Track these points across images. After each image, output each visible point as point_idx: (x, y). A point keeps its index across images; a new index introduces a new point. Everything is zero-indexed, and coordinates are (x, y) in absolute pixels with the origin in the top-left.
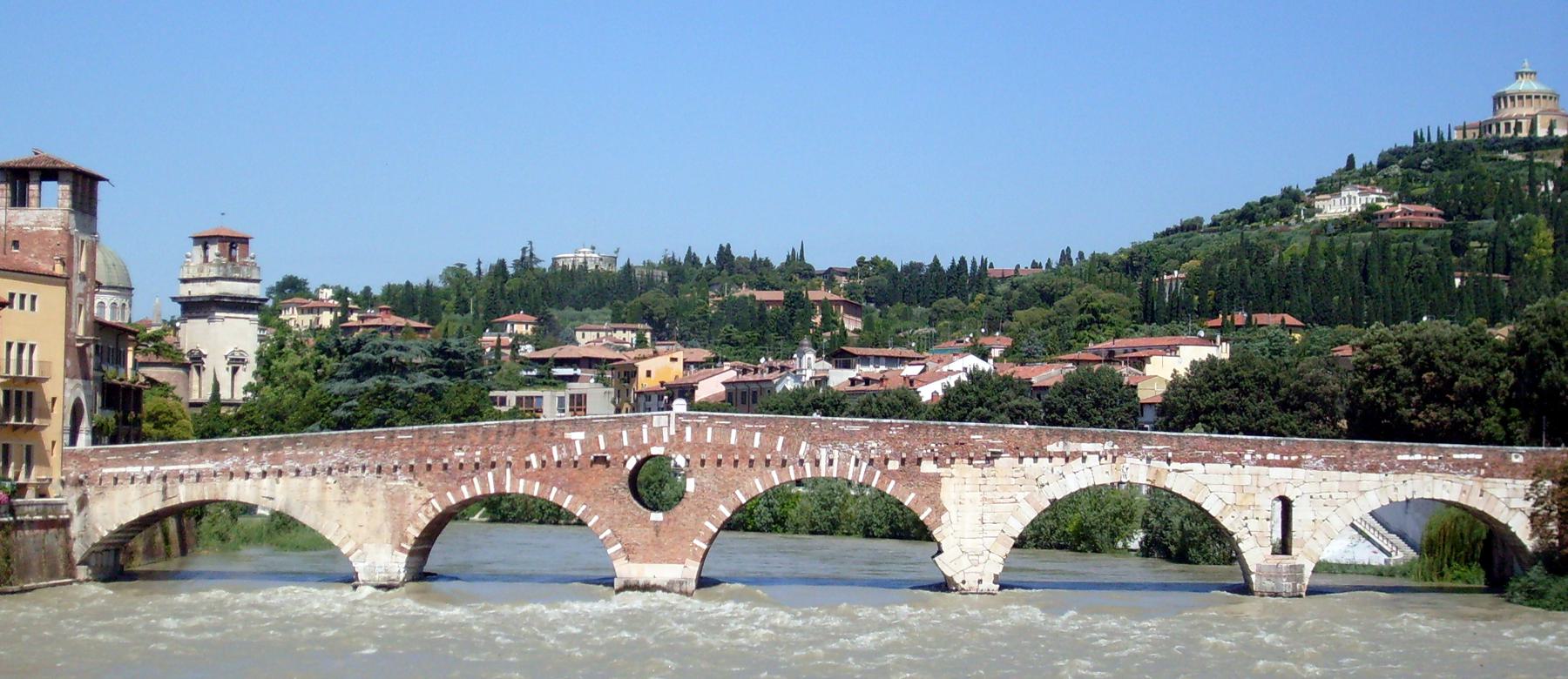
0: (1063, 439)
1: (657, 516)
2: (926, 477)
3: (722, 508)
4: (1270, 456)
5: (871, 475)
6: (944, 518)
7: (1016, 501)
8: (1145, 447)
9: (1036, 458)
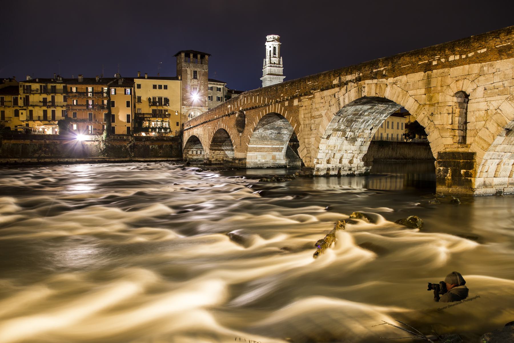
0: (339, 76)
4: (451, 58)
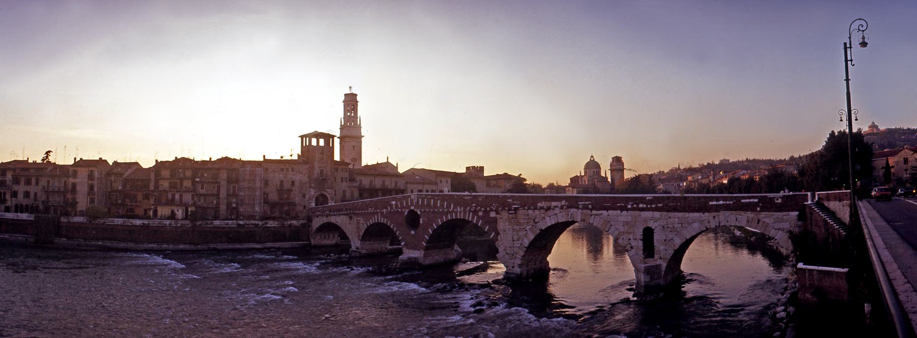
1: (413, 232)
3: (430, 230)
4: (641, 206)
5: (473, 218)
6: (499, 237)
7: (526, 230)
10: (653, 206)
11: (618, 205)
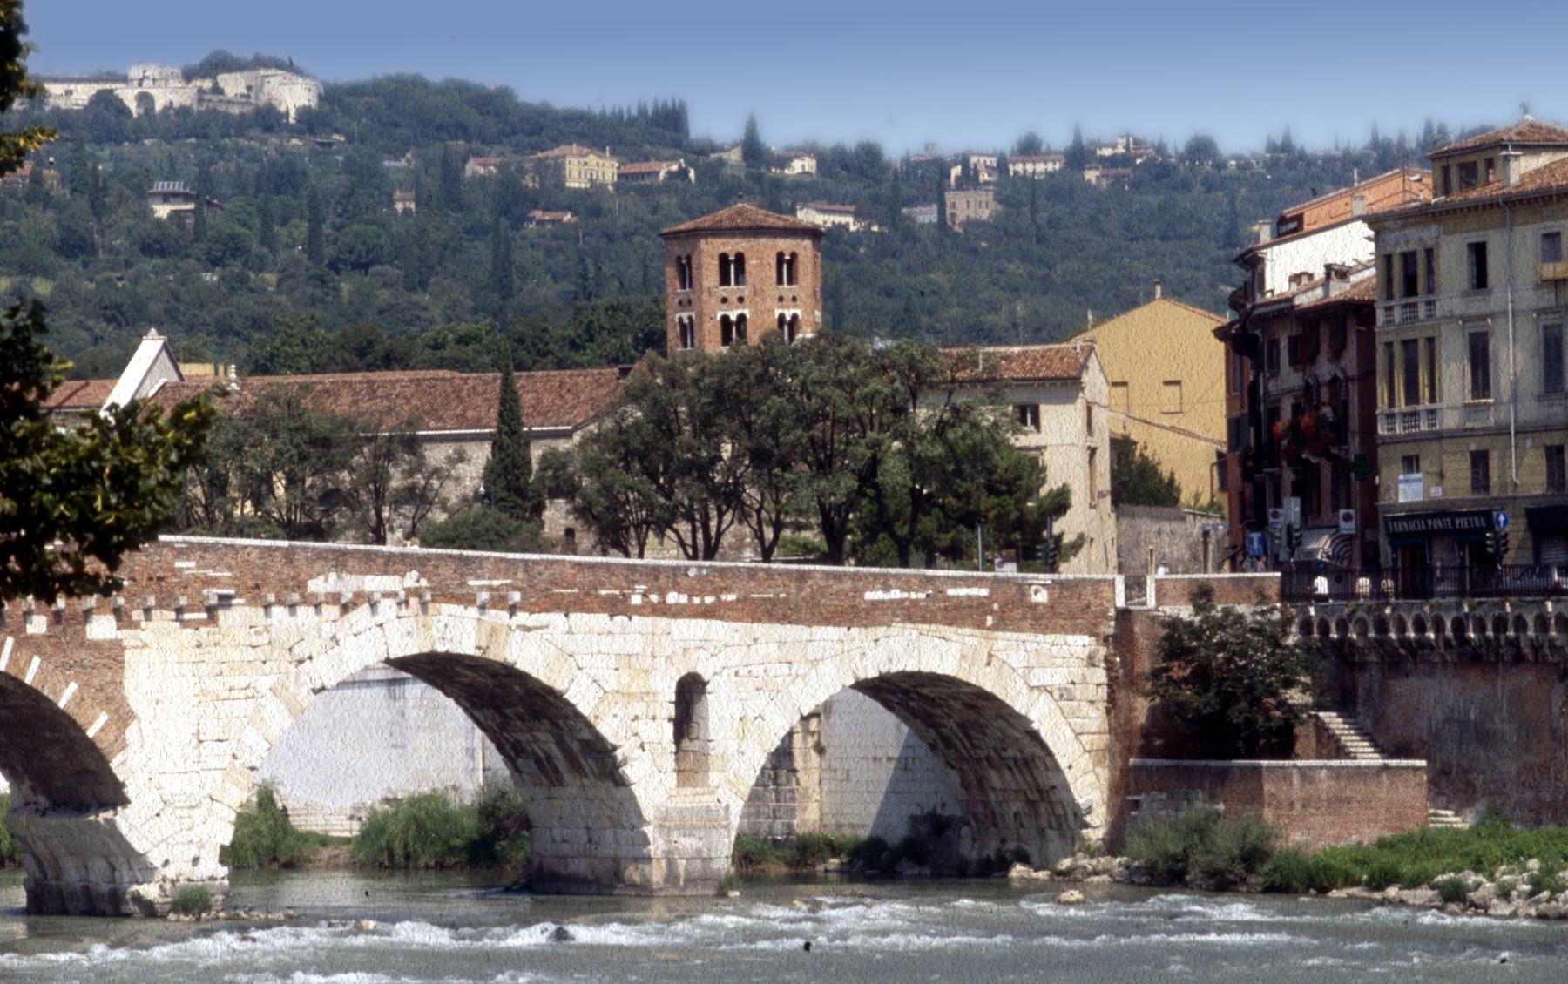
2: (97, 646)
4: (673, 598)
6: (131, 732)
8: (472, 582)
9: (292, 607)
10: (709, 600)
11: (603, 592)
